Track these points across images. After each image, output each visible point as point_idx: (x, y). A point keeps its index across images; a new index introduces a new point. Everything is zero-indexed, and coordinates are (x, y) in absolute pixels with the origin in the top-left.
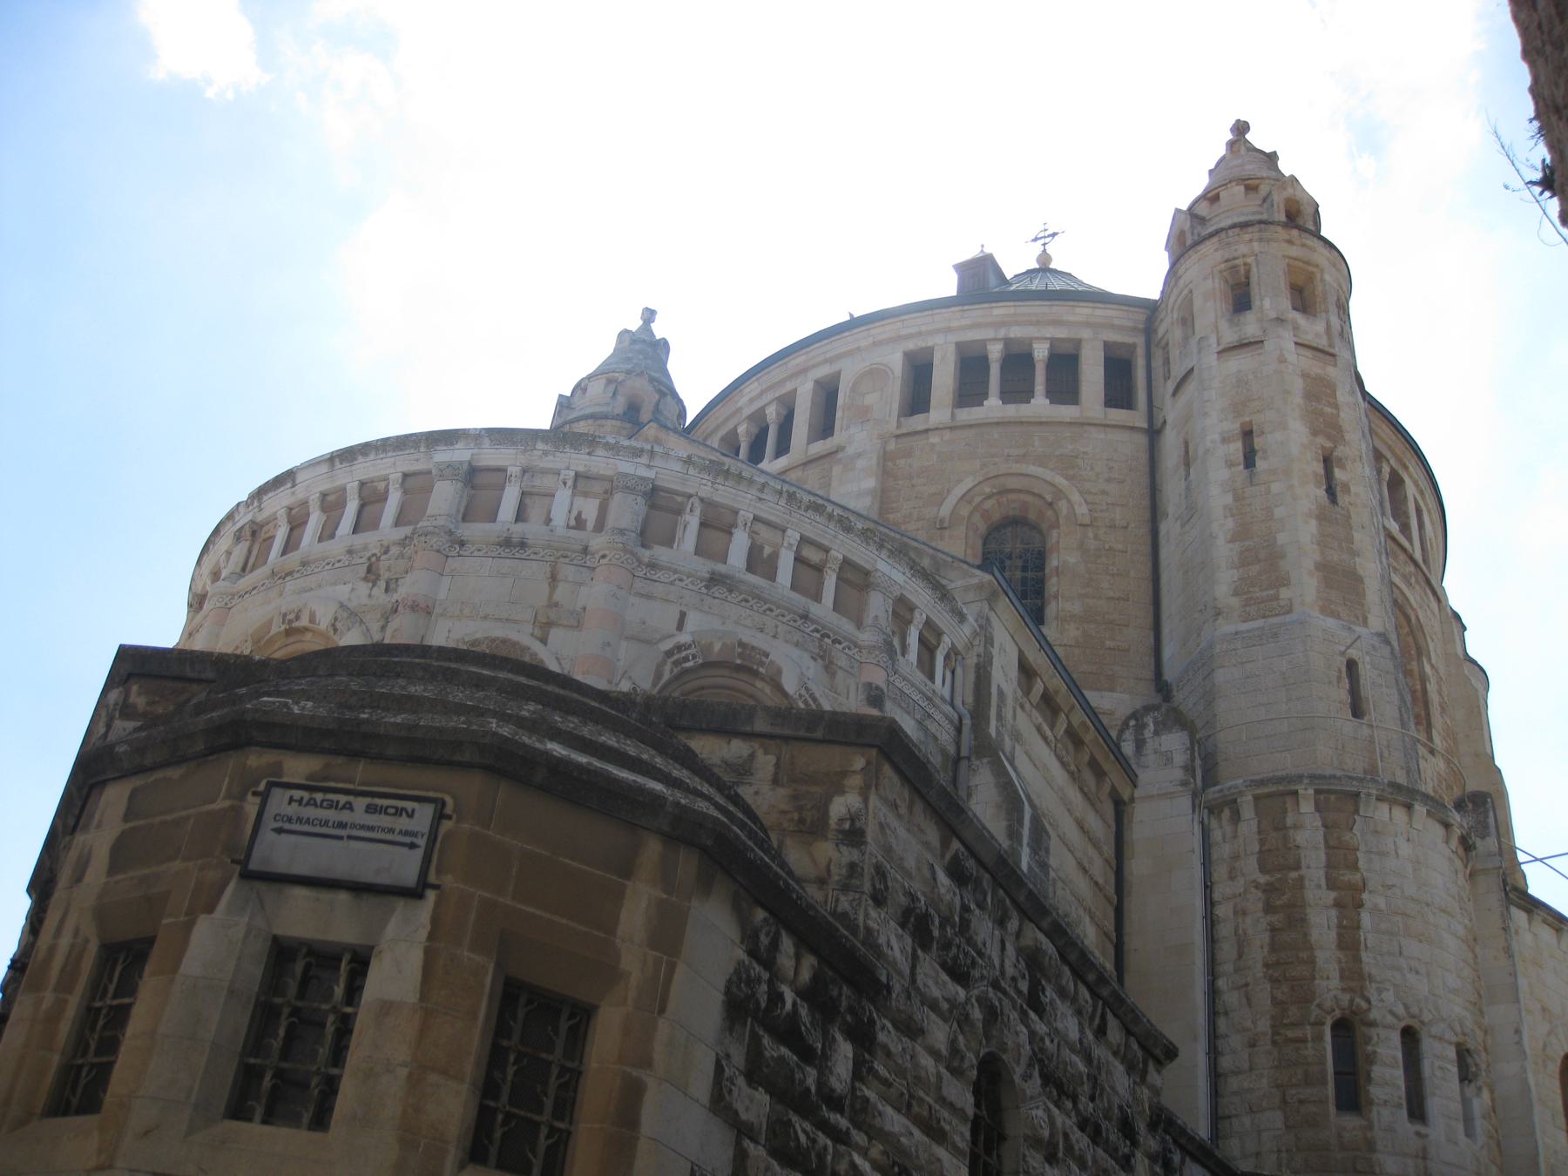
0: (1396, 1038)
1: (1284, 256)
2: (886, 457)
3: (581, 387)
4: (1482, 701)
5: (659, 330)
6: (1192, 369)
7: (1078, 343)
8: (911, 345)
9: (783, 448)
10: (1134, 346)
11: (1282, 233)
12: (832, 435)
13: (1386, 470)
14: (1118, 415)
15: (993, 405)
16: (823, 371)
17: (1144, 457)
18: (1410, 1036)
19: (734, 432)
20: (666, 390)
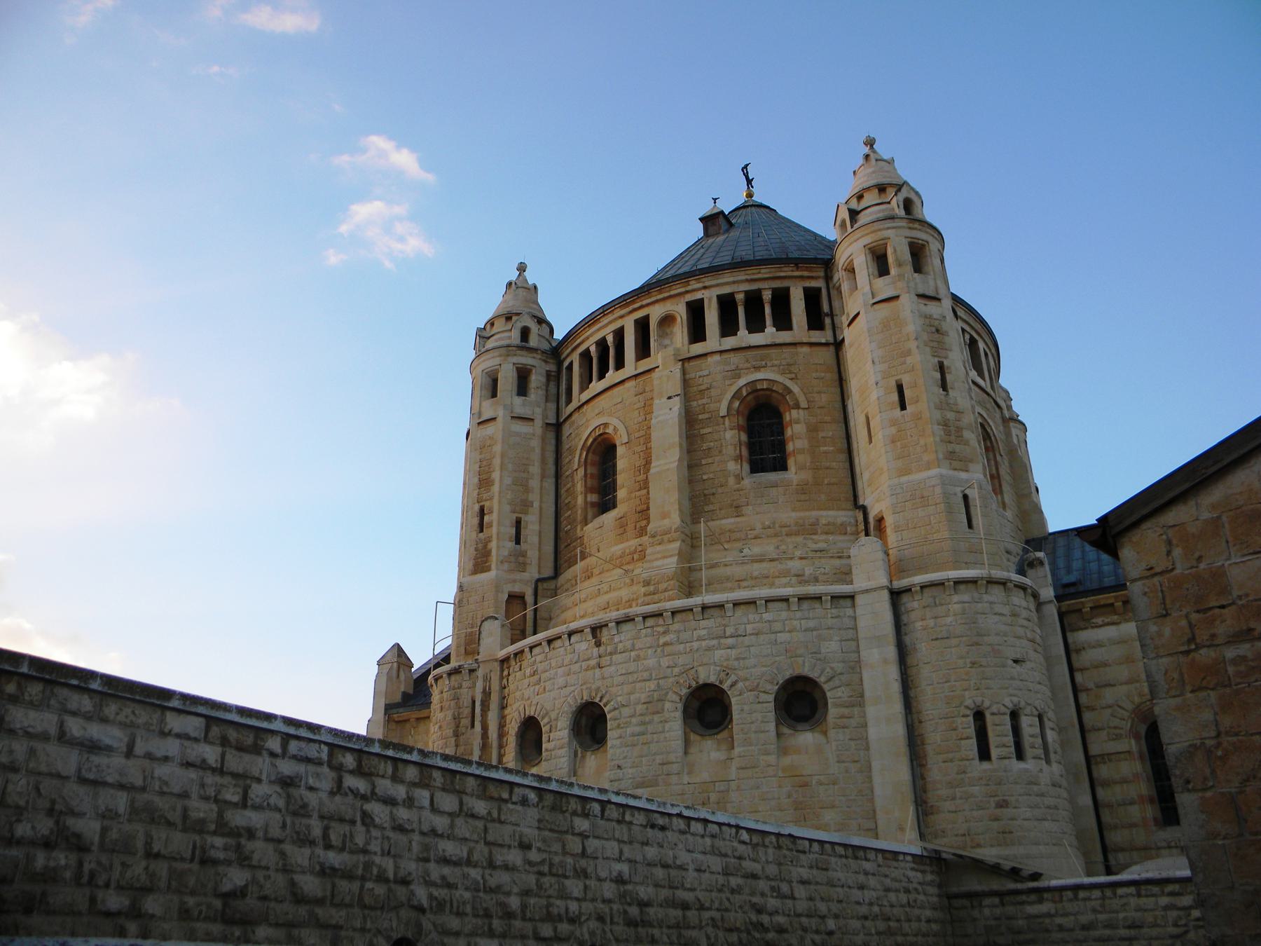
0: (1008, 718)
1: (906, 237)
2: (684, 372)
3: (491, 323)
4: (1027, 463)
5: (531, 277)
6: (858, 314)
7: (786, 291)
8: (689, 298)
9: (620, 364)
10: (819, 289)
11: (903, 223)
12: (650, 356)
13: (967, 337)
14: (817, 336)
15: (744, 337)
16: (639, 314)
17: (834, 362)
18: (1014, 715)
19: (587, 351)
20: (542, 321)
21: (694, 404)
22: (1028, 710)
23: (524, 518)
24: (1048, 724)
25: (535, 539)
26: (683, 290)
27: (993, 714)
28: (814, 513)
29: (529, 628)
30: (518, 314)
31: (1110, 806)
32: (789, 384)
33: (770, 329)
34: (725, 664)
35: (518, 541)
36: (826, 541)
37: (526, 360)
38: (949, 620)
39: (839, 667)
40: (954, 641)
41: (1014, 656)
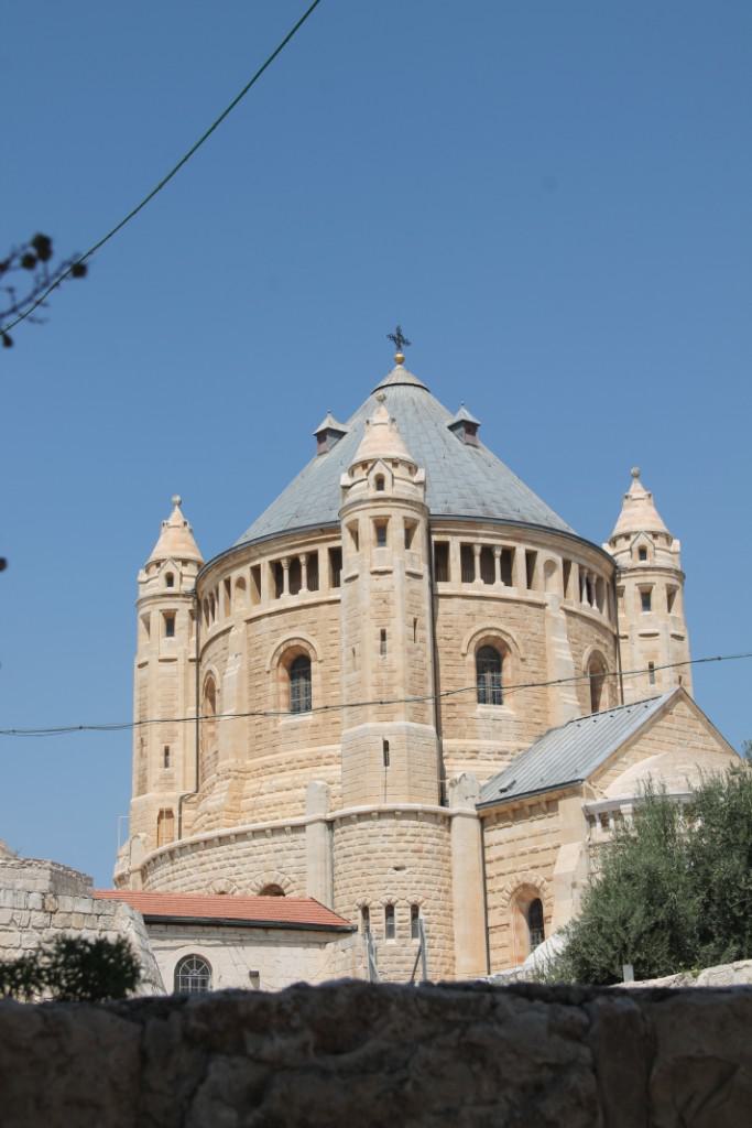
15: (288, 599)
18: (390, 910)
21: (253, 659)
22: (400, 903)
23: (172, 747)
24: (421, 910)
25: (181, 762)
26: (246, 557)
27: (373, 909)
28: (323, 748)
29: (177, 837)
30: (164, 560)
31: (496, 964)
32: (310, 639)
33: (304, 590)
34: (231, 877)
35: (166, 765)
36: (325, 771)
37: (169, 605)
38: (351, 843)
39: (293, 876)
40: (354, 857)
41: (397, 865)
